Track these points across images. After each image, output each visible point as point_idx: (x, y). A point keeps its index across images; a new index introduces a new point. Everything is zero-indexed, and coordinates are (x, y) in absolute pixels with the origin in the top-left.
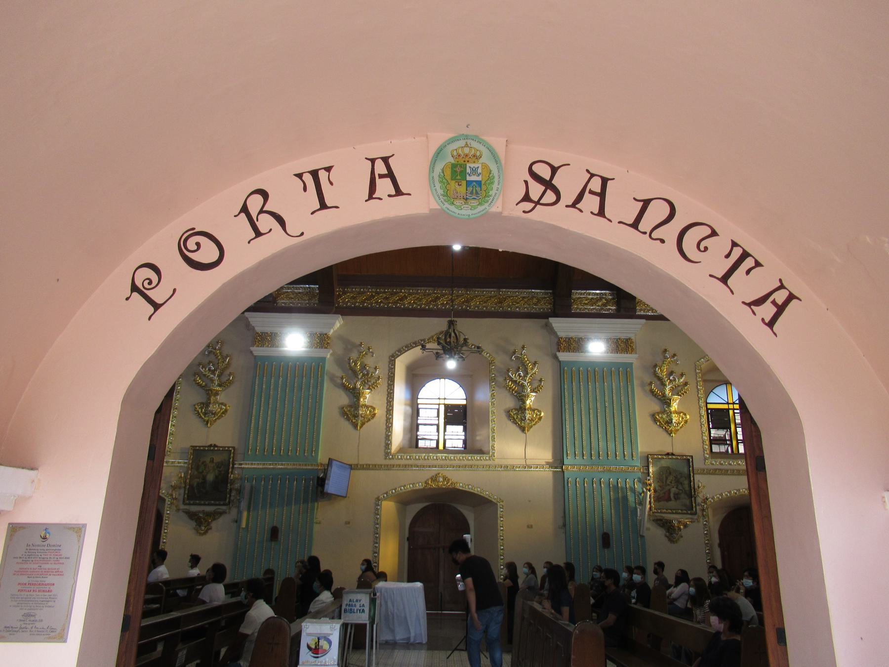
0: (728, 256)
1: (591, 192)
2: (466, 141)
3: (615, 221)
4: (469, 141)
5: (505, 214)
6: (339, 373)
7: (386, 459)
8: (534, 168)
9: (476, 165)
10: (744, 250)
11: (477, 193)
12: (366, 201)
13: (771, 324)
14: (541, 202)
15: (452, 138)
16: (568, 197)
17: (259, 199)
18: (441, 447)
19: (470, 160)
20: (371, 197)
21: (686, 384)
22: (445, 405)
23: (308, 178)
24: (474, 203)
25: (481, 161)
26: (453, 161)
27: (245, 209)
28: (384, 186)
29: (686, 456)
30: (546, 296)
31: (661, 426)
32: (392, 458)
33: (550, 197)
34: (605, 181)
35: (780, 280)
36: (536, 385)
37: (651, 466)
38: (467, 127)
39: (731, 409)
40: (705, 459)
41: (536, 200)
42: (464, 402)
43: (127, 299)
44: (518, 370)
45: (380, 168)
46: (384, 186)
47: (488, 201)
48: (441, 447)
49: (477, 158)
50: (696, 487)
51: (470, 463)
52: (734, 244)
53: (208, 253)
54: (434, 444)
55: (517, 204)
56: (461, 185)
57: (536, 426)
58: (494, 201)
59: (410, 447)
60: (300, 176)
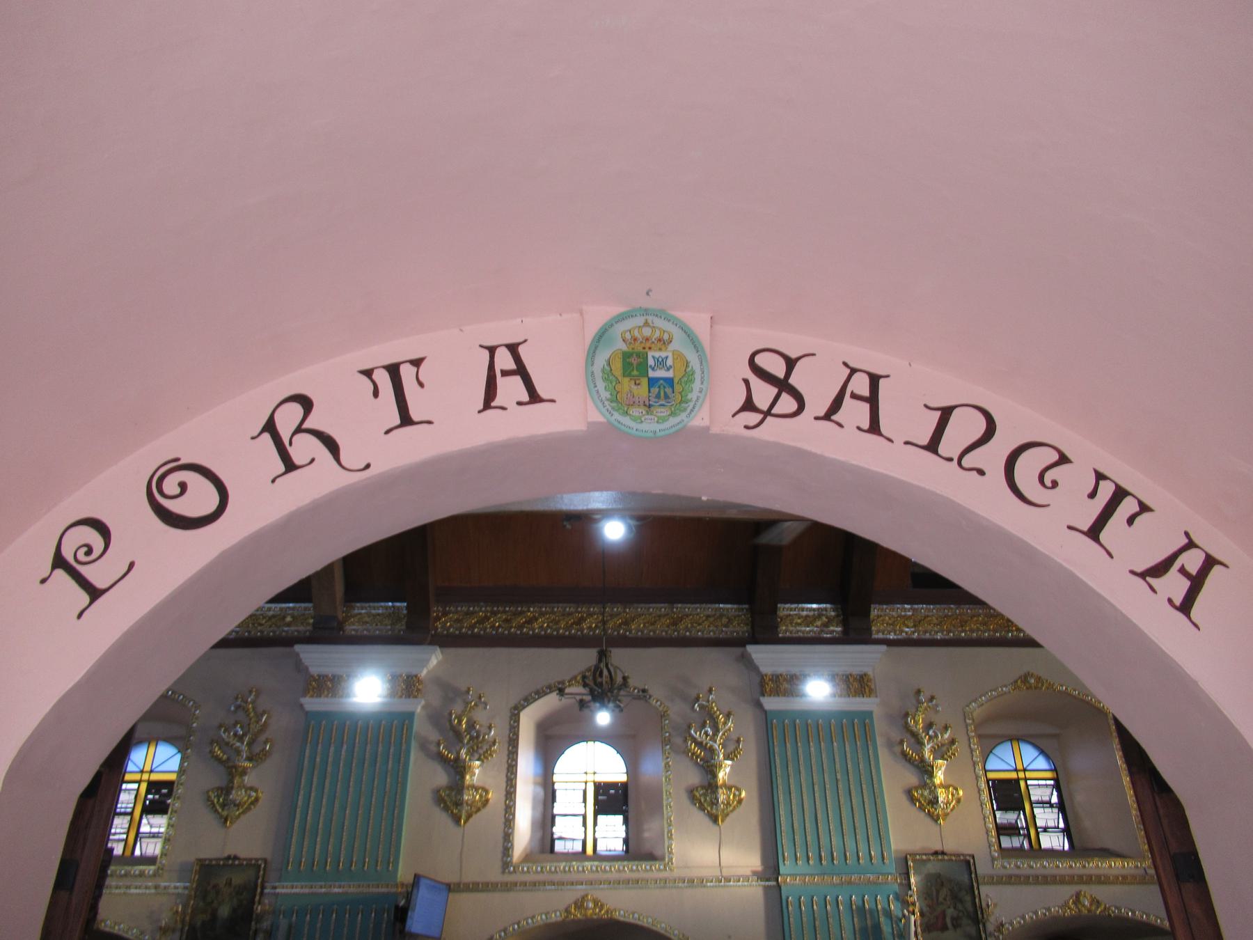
0: (1092, 495)
1: (854, 396)
2: (645, 317)
3: (899, 441)
4: (650, 318)
5: (715, 430)
6: (433, 735)
7: (503, 872)
8: (759, 360)
9: (663, 354)
10: (1117, 486)
11: (666, 397)
12: (479, 412)
13: (1186, 607)
14: (774, 411)
15: (619, 315)
16: (817, 403)
17: (296, 410)
18: (589, 850)
19: (653, 345)
20: (488, 404)
21: (953, 742)
22: (595, 783)
23: (383, 378)
24: (663, 412)
25: (671, 347)
26: (624, 347)
27: (270, 427)
28: (511, 389)
29: (963, 855)
30: (740, 613)
31: (922, 808)
32: (515, 871)
33: (787, 404)
34: (874, 380)
35: (1187, 534)
36: (731, 747)
37: (912, 872)
38: (648, 294)
39: (1022, 779)
40: (993, 859)
41: (765, 407)
42: (623, 778)
43: (43, 581)
44: (704, 726)
46: (511, 389)
47: (685, 410)
48: (589, 850)
49: (663, 342)
50: (984, 905)
51: (635, 875)
52: (1100, 477)
53: (200, 499)
54: (578, 848)
55: (733, 416)
56: (639, 384)
57: (735, 812)
58: (696, 409)
59: (542, 851)
60: (368, 373)
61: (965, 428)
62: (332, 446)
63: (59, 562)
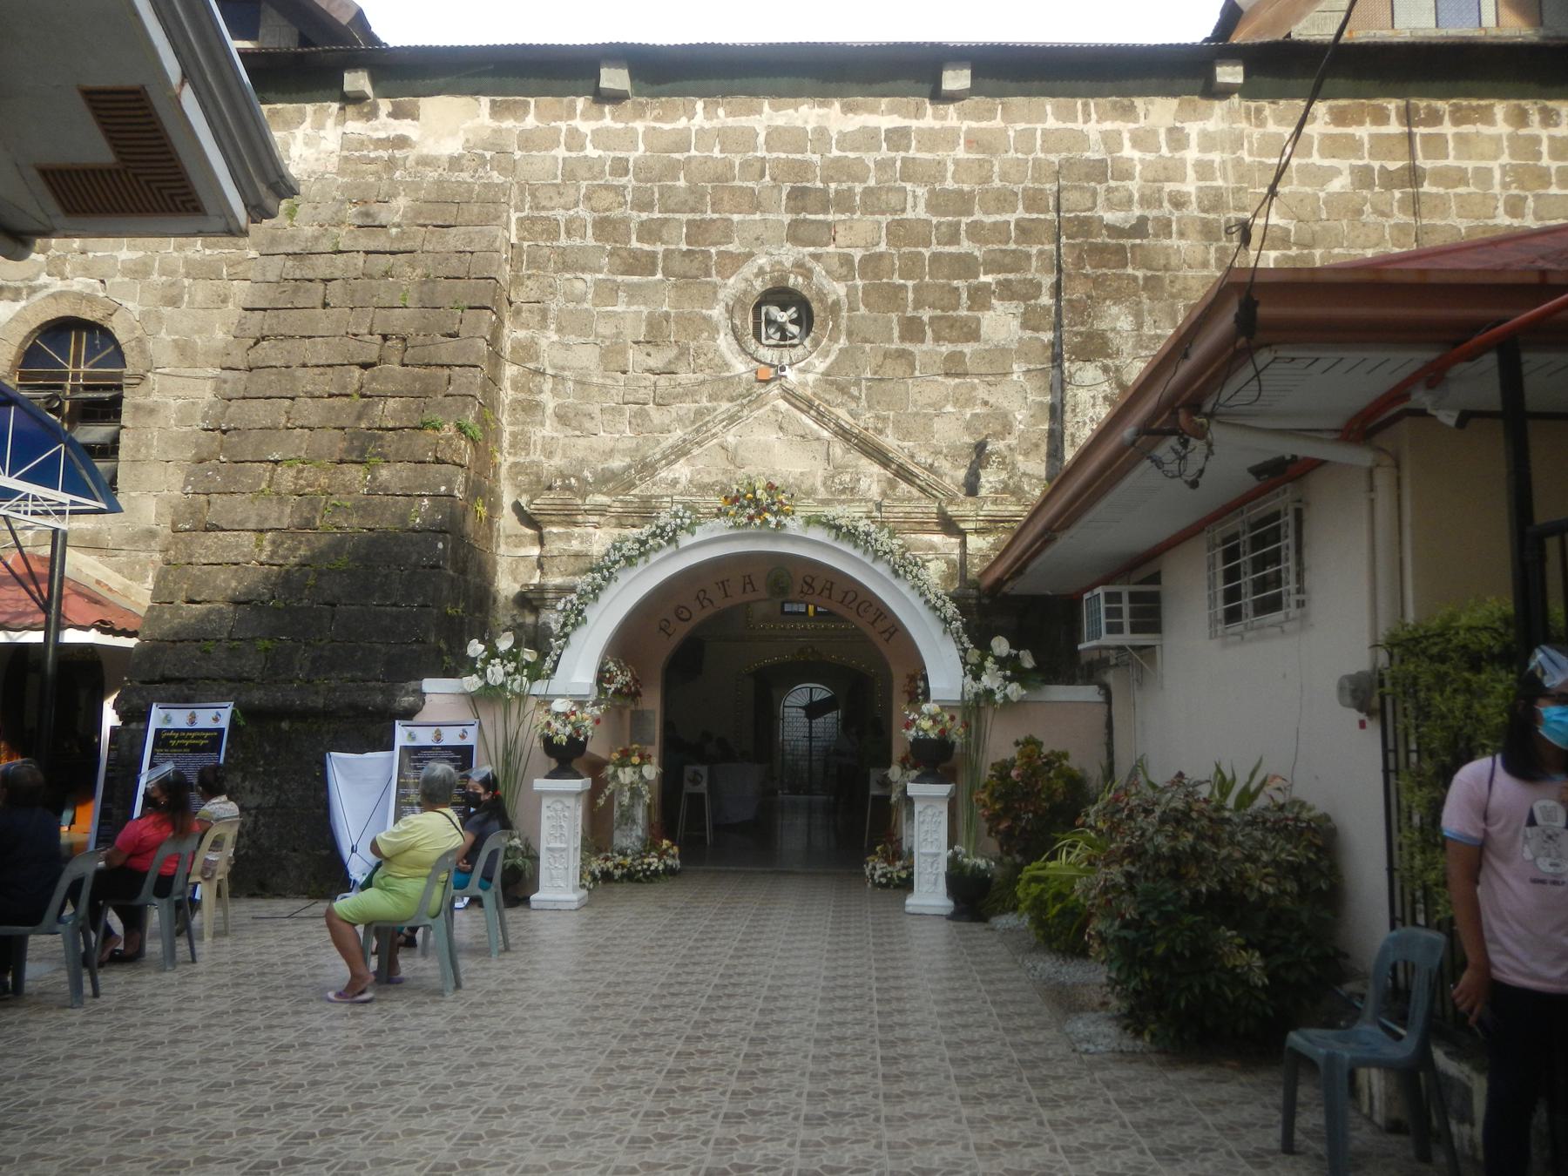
13: (887, 641)
16: (818, 590)
27: (698, 597)
46: (749, 587)
53: (685, 615)
61: (851, 597)
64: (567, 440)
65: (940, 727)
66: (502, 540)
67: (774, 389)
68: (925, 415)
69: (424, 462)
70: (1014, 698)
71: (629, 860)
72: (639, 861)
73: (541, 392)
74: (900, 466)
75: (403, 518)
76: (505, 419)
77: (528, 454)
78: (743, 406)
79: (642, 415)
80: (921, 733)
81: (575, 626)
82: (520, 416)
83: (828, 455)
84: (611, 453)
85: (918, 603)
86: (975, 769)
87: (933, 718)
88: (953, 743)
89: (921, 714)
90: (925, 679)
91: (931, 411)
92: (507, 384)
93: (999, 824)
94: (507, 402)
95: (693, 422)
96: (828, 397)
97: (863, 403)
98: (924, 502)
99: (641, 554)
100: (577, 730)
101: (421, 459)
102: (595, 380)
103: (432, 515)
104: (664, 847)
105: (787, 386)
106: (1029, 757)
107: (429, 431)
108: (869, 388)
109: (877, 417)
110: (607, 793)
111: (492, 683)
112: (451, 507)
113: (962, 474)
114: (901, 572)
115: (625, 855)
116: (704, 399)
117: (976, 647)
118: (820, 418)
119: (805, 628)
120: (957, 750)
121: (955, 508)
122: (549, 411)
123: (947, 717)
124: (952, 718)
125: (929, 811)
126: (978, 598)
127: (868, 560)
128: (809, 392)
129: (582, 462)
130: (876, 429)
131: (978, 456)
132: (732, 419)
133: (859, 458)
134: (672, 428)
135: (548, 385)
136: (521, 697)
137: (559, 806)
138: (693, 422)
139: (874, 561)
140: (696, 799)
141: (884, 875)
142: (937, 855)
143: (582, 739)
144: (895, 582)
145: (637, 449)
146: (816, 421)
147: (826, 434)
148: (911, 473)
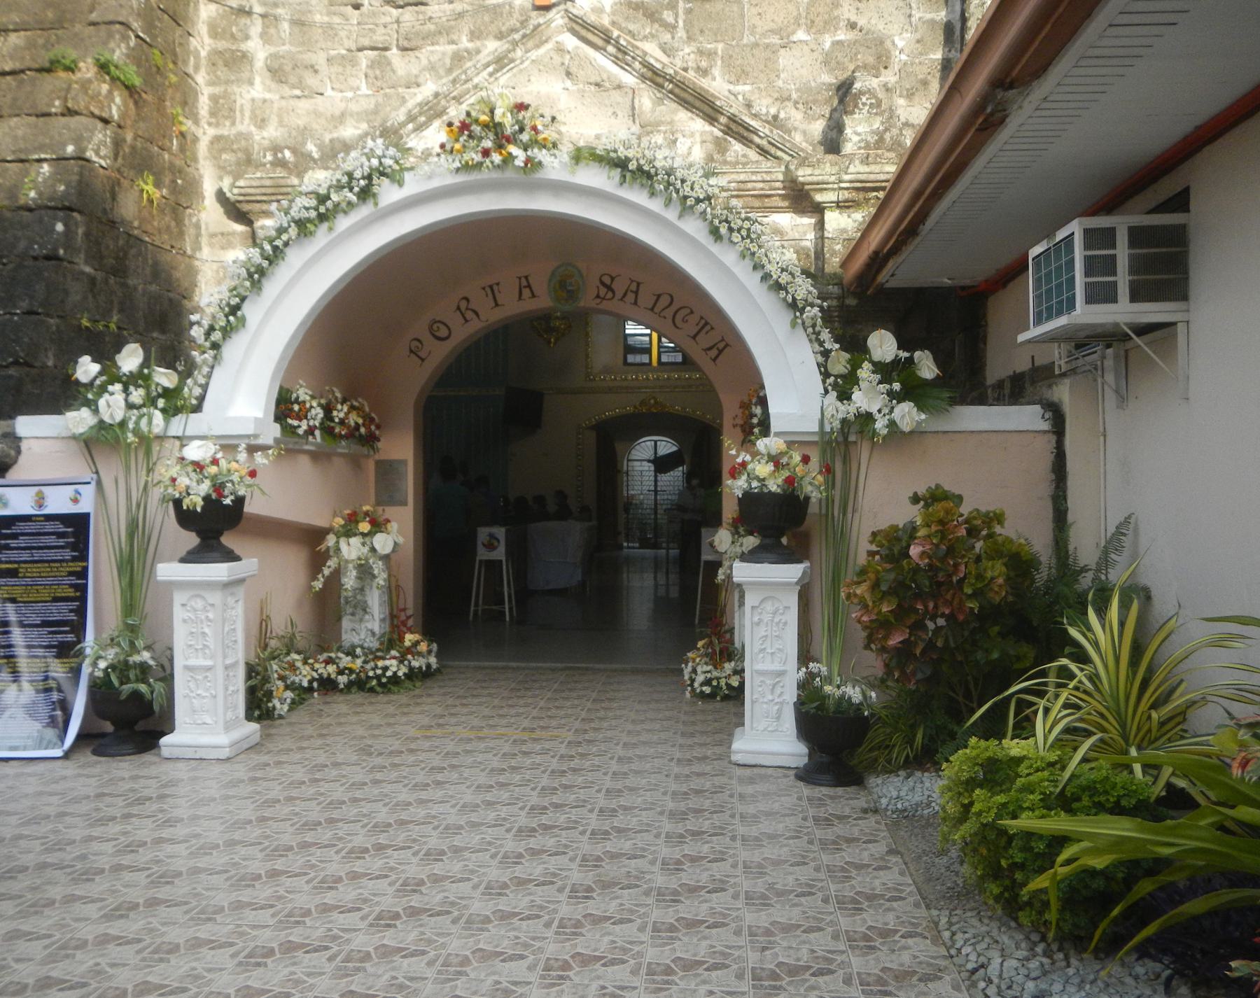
13: (714, 360)
16: (619, 294)
20: (520, 298)
27: (459, 308)
28: (526, 292)
33: (610, 295)
34: (638, 284)
45: (524, 283)
46: (526, 292)
53: (443, 332)
54: (645, 359)
61: (664, 301)
62: (477, 314)
63: (411, 351)
64: (283, 103)
65: (786, 474)
66: (204, 240)
67: (557, 18)
68: (767, 46)
69: (48, 115)
70: (906, 426)
71: (359, 662)
72: (372, 664)
73: (247, 37)
74: (732, 119)
75: (13, 192)
76: (201, 78)
77: (233, 123)
78: (515, 44)
79: (381, 65)
80: (755, 484)
81: (227, 331)
82: (222, 72)
83: (633, 108)
84: (341, 118)
85: (752, 281)
86: (840, 539)
87: (775, 460)
88: (807, 499)
89: (755, 454)
90: (763, 402)
91: (775, 40)
92: (202, 29)
93: (886, 638)
94: (203, 54)
95: (450, 71)
96: (631, 27)
97: (681, 33)
98: (766, 165)
99: (322, 218)
100: (219, 488)
101: (45, 110)
102: (318, 18)
103: (53, 186)
104: (407, 643)
105: (575, 11)
106: (941, 522)
107: (62, 74)
108: (689, 12)
109: (701, 52)
110: (326, 572)
111: (107, 419)
112: (81, 174)
113: (818, 127)
114: (723, 230)
115: (355, 656)
116: (464, 39)
117: (843, 348)
118: (622, 56)
119: (647, 378)
120: (813, 509)
121: (809, 171)
122: (259, 63)
123: (797, 458)
124: (806, 460)
125: (769, 607)
126: (841, 298)
127: (671, 215)
128: (606, 21)
129: (305, 132)
130: (698, 69)
131: (841, 101)
132: (501, 62)
133: (675, 112)
134: (421, 80)
135: (256, 28)
136: (146, 442)
137: (199, 604)
138: (450, 71)
139: (680, 216)
140: (493, 566)
141: (707, 682)
142: (781, 674)
143: (228, 501)
144: (715, 248)
145: (376, 112)
146: (616, 60)
147: (629, 79)
148: (747, 128)
